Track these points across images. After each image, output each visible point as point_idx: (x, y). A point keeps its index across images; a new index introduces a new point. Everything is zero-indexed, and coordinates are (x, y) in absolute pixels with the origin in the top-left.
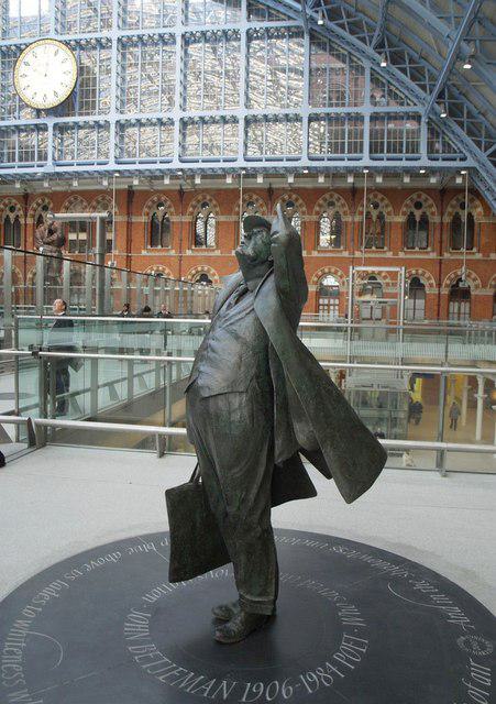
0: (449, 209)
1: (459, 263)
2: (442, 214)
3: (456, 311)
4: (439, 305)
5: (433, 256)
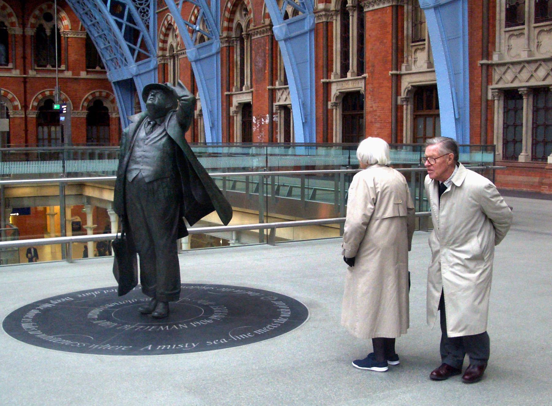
0: (32, 20)
1: (50, 83)
2: (23, 25)
3: (46, 136)
4: (26, 131)
5: (16, 73)
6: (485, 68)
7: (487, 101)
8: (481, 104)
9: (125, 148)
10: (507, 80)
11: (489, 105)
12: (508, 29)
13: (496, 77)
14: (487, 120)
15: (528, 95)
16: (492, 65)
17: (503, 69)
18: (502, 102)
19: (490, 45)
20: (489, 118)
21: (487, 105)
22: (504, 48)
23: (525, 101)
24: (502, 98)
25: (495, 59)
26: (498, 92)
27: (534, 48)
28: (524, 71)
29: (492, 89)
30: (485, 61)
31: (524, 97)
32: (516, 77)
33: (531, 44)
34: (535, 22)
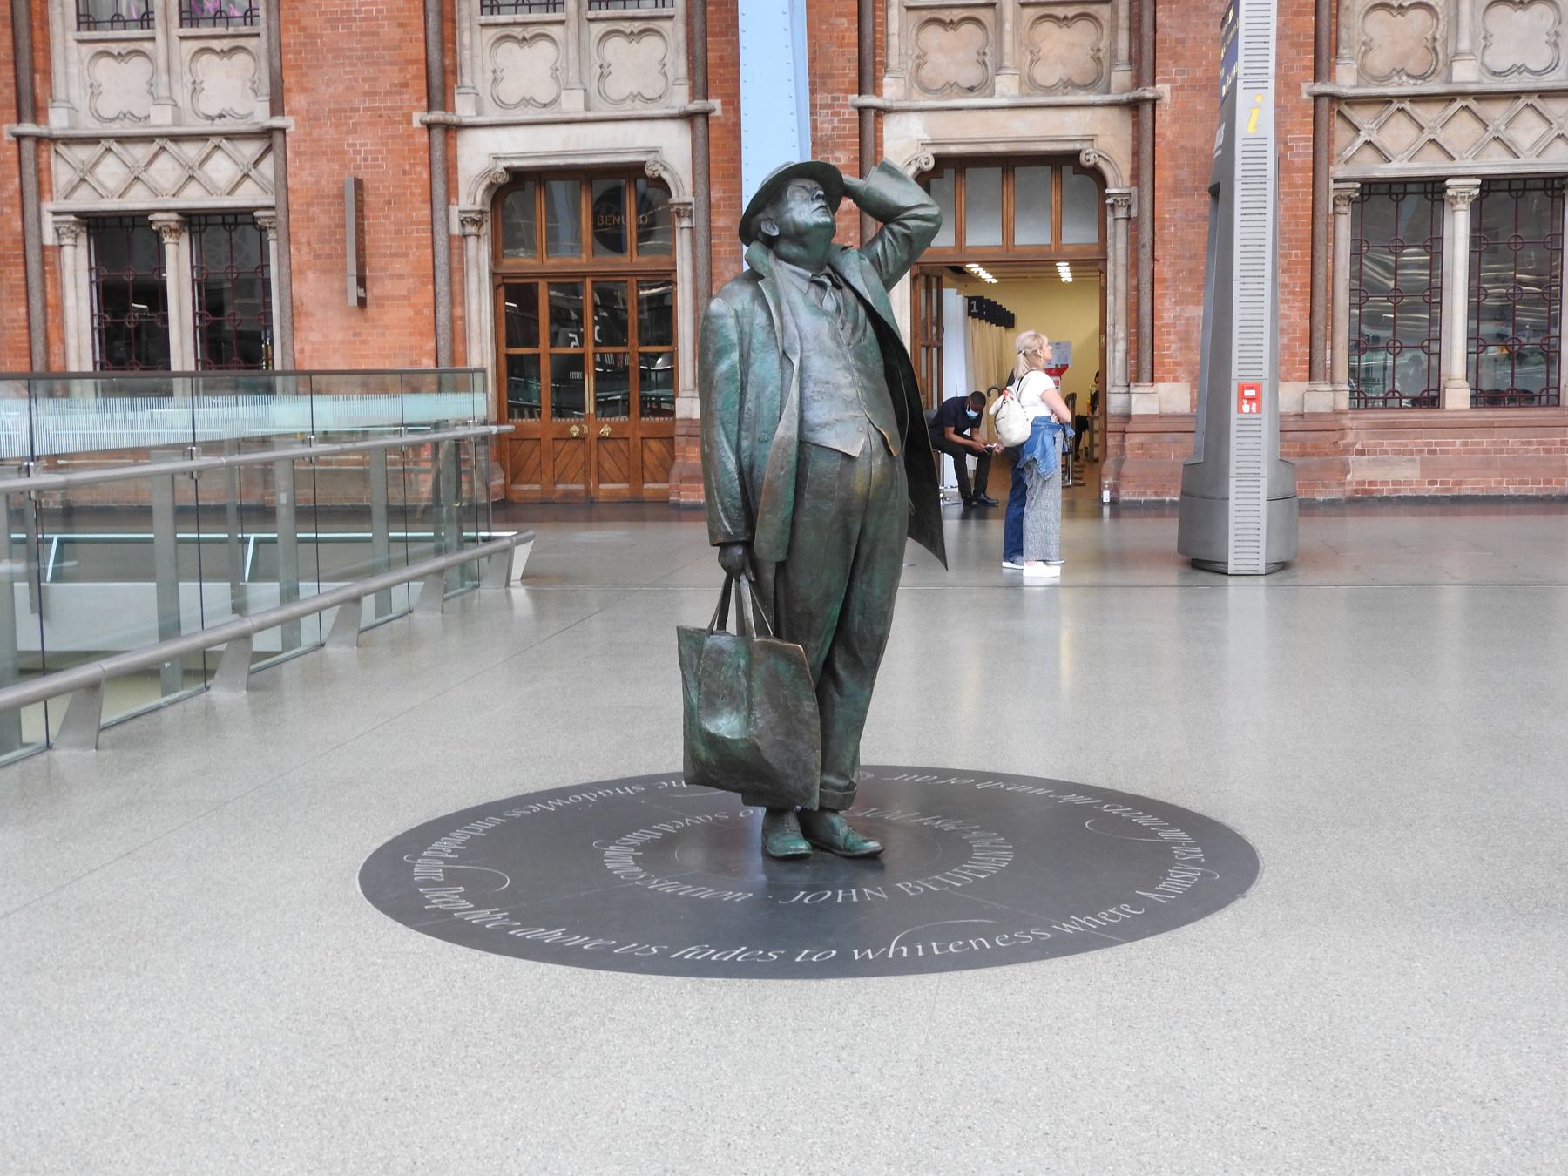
6: (28, 145)
7: (43, 248)
8: (25, 256)
9: (745, 359)
10: (111, 185)
11: (49, 258)
12: (86, 35)
13: (62, 174)
14: (45, 306)
15: (176, 232)
16: (53, 140)
17: (83, 154)
18: (83, 252)
19: (38, 77)
20: (51, 299)
21: (43, 262)
22: (78, 93)
23: (170, 250)
24: (83, 240)
25: (57, 121)
26: (75, 223)
27: (183, 96)
28: (164, 162)
29: (55, 213)
30: (28, 128)
31: (167, 239)
32: (137, 178)
33: (177, 88)
34: (181, 26)
